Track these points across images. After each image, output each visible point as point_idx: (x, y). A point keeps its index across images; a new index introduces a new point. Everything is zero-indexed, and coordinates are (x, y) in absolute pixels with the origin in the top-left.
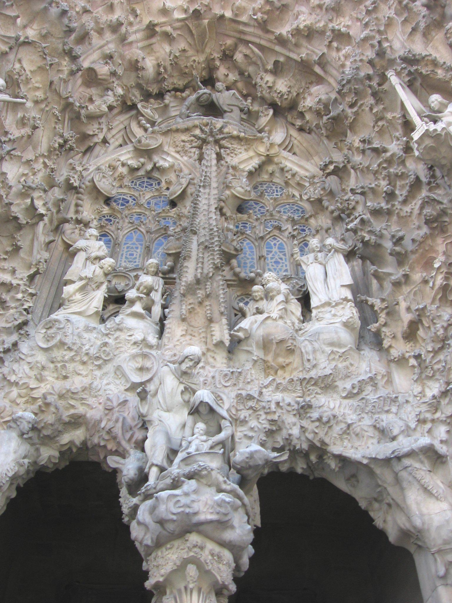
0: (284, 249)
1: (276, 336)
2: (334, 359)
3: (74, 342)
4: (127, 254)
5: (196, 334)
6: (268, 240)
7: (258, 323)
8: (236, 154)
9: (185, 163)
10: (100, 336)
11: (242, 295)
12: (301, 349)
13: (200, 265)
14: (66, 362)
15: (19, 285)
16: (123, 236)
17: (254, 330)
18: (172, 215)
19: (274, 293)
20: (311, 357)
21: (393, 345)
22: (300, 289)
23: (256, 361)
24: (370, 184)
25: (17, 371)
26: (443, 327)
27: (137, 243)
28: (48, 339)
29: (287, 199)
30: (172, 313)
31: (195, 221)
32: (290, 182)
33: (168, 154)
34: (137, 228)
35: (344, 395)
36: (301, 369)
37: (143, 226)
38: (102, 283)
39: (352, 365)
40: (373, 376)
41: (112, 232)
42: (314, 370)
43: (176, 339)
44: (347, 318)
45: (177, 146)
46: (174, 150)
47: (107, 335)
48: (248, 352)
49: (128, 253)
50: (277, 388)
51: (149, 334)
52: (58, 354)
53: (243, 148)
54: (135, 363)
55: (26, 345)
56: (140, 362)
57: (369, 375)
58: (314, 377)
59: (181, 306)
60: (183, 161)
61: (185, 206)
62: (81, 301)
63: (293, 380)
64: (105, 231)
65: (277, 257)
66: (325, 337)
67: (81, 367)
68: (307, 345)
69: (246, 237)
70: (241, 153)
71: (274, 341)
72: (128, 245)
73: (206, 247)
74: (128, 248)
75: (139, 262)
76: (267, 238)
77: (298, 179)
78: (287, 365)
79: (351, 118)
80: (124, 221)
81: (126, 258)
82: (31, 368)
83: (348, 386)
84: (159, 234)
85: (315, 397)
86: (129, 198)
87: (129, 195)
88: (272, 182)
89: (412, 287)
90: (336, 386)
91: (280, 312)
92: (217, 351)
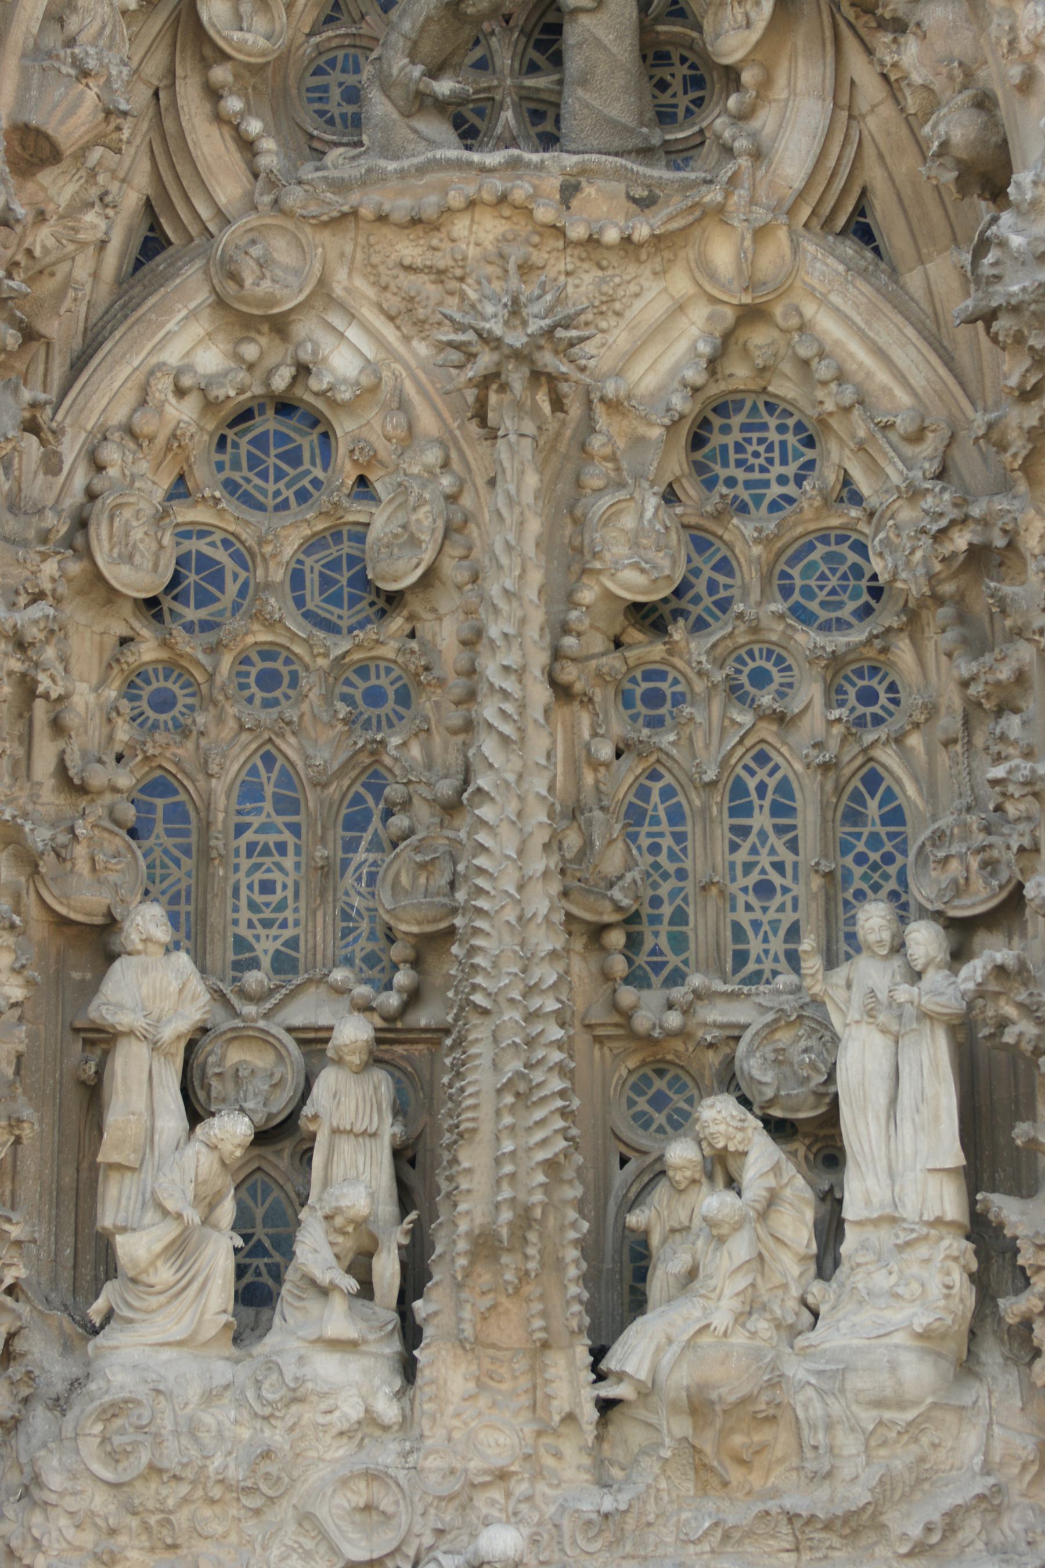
0: (791, 811)
1: (724, 1391)
2: (884, 1444)
3: (185, 1460)
4: (250, 887)
7: (676, 1348)
8: (618, 314)
9: (422, 377)
11: (644, 1064)
12: (794, 1410)
13: (506, 1193)
14: (171, 1512)
16: (228, 795)
17: (662, 1376)
18: (391, 655)
19: (725, 1230)
22: (822, 1089)
23: (667, 1460)
25: (45, 1542)
27: (279, 820)
28: (114, 1457)
29: (817, 519)
30: (436, 1321)
31: (480, 949)
32: (833, 422)
33: (352, 317)
34: (270, 740)
35: (904, 1550)
36: (794, 1461)
37: (292, 740)
39: (935, 1446)
40: (987, 1492)
41: (184, 772)
42: (827, 1483)
43: (450, 1410)
45: (385, 288)
46: (371, 292)
47: (266, 1418)
48: (649, 1425)
49: (259, 876)
50: (726, 1537)
52: (148, 1493)
53: (647, 271)
54: (349, 1495)
55: (55, 1463)
56: (360, 1493)
57: (981, 1485)
58: (821, 1515)
59: (459, 1304)
60: (413, 363)
61: (434, 610)
63: (767, 1513)
64: (160, 767)
65: (764, 860)
66: (860, 1385)
67: (207, 1512)
68: (810, 1400)
69: (658, 761)
70: (637, 295)
71: (718, 1408)
72: (249, 836)
73: (518, 1095)
74: (251, 847)
75: (297, 923)
76: (733, 761)
77: (862, 433)
79: (1015, 456)
80: (220, 720)
81: (253, 906)
82: (78, 1527)
83: (916, 1531)
84: (353, 774)
85: (826, 1557)
86: (221, 555)
87: (217, 537)
88: (764, 390)
90: (884, 1526)
91: (736, 1304)
92: (564, 1430)
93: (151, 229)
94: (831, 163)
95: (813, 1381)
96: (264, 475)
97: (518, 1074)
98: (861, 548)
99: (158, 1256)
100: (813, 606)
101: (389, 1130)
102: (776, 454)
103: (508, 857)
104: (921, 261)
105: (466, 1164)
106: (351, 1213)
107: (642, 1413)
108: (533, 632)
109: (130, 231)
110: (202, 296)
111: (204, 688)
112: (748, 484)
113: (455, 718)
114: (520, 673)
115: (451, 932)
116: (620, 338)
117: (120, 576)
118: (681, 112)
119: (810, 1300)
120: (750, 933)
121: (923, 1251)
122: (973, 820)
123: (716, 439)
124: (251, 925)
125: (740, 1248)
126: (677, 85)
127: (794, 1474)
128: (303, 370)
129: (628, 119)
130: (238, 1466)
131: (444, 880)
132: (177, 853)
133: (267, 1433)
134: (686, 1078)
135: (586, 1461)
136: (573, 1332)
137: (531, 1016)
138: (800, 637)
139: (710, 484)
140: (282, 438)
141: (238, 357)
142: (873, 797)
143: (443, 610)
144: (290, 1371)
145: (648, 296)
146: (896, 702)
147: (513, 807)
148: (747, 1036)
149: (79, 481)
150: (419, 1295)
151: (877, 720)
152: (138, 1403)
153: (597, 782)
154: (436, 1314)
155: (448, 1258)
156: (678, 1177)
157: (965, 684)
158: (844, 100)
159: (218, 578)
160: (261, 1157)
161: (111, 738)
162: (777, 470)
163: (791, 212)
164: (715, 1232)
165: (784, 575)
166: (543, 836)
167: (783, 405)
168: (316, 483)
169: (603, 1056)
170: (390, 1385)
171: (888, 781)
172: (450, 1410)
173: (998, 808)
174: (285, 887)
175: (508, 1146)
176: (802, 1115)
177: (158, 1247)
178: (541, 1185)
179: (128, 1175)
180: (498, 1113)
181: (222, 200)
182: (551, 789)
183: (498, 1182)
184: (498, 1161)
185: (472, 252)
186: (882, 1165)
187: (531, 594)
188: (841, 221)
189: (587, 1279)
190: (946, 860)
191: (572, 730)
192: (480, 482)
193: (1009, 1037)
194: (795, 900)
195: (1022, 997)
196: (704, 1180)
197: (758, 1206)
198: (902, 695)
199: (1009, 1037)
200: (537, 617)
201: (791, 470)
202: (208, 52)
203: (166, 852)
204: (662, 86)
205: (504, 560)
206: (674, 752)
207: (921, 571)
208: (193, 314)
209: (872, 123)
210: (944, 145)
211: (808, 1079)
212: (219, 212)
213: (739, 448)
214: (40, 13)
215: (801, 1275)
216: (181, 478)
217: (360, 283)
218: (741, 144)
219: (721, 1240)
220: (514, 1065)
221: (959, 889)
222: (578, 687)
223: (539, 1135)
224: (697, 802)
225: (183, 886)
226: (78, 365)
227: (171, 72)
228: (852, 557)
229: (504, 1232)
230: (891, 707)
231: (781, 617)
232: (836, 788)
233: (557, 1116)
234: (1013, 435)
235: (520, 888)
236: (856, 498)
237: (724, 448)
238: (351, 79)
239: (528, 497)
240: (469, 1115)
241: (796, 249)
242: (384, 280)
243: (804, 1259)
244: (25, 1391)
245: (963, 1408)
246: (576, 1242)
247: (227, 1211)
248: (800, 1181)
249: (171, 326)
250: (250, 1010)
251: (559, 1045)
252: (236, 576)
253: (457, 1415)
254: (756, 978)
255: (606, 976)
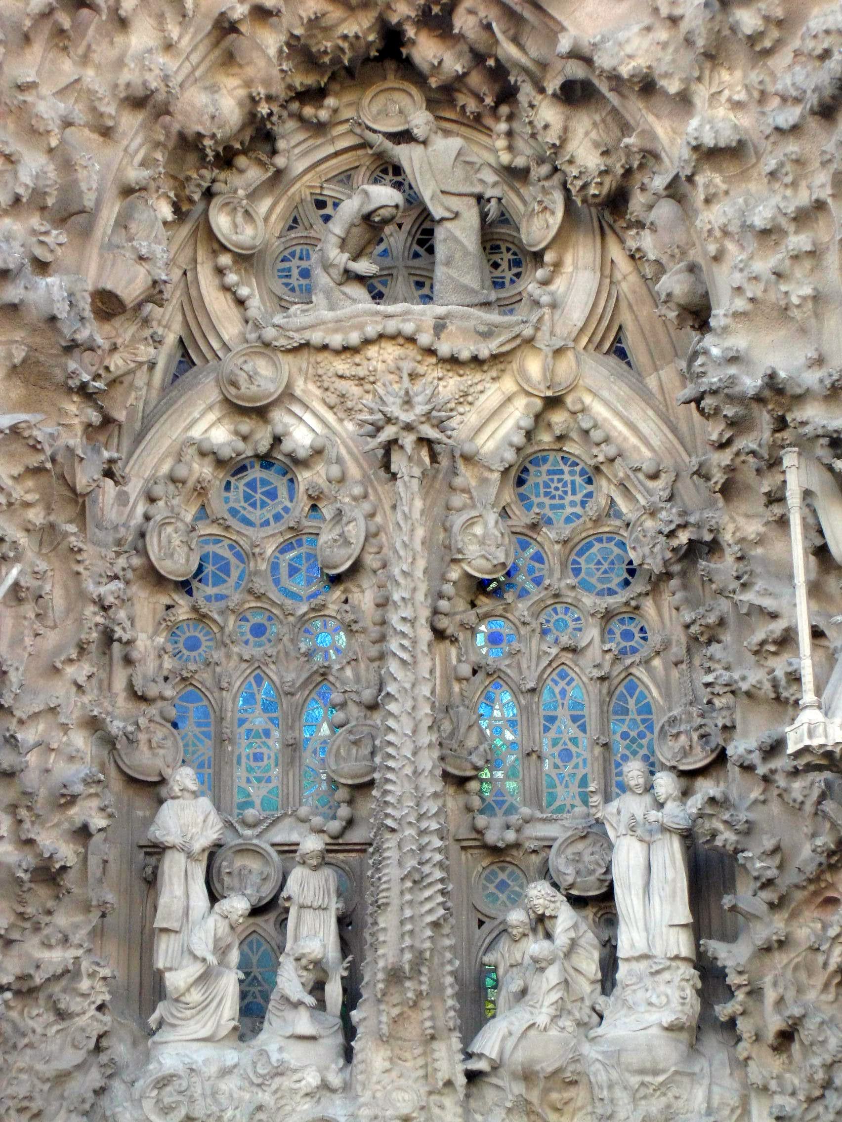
1: (544, 1065)
2: (645, 1097)
5: (408, 1055)
6: (549, 682)
8: (471, 404)
9: (351, 444)
10: (247, 1084)
15: (77, 958)
18: (334, 614)
19: (543, 965)
20: (605, 1094)
21: (754, 1055)
22: (602, 877)
24: (744, 678)
26: (824, 1065)
30: (365, 1023)
31: (390, 791)
32: (603, 467)
33: (307, 407)
36: (589, 1109)
37: (273, 667)
38: (229, 947)
39: (676, 1098)
41: (207, 689)
44: (669, 1020)
45: (327, 389)
46: (318, 392)
47: (259, 1085)
48: (498, 1087)
51: (327, 1068)
53: (488, 376)
59: (380, 1012)
60: (344, 435)
61: (359, 586)
62: (203, 1007)
64: (191, 684)
68: (598, 1070)
70: (482, 392)
71: (541, 1075)
73: (415, 882)
76: (545, 676)
77: (621, 474)
78: (566, 1103)
80: (228, 656)
81: (250, 770)
84: (311, 687)
86: (227, 554)
88: (561, 450)
89: (792, 955)
91: (552, 1011)
92: (446, 1091)
93: (183, 356)
94: (600, 310)
95: (600, 1058)
96: (254, 505)
97: (414, 868)
98: (622, 545)
99: (192, 985)
100: (593, 581)
101: (335, 906)
102: (569, 489)
103: (406, 735)
104: (656, 369)
105: (382, 925)
106: (312, 957)
107: (494, 1080)
108: (420, 596)
109: (170, 357)
110: (214, 396)
111: (218, 635)
112: (553, 507)
113: (374, 651)
114: (412, 622)
115: (371, 784)
116: (473, 418)
117: (165, 567)
118: (507, 281)
119: (598, 1008)
120: (557, 782)
121: (666, 976)
122: (694, 710)
123: (531, 480)
124: (248, 781)
125: (553, 975)
126: (504, 265)
127: (589, 1117)
128: (277, 440)
129: (476, 286)
130: (242, 1116)
131: (366, 751)
132: (202, 736)
133: (260, 1094)
134: (517, 871)
135: (459, 1110)
136: (450, 1030)
137: (422, 833)
138: (584, 600)
139: (529, 507)
140: (264, 482)
141: (237, 433)
142: (631, 697)
143: (365, 586)
144: (275, 1057)
145: (488, 393)
146: (644, 639)
147: (409, 704)
148: (556, 845)
149: (140, 510)
150: (354, 1007)
151: (634, 651)
152: (179, 1077)
153: (461, 689)
154: (365, 1019)
155: (372, 983)
156: (515, 932)
157: (687, 627)
158: (607, 272)
159: (226, 569)
160: (254, 924)
161: (161, 666)
162: (569, 498)
163: (576, 340)
164: (538, 966)
165: (575, 562)
166: (428, 722)
167: (573, 459)
168: (286, 510)
169: (467, 859)
170: (336, 1063)
171: (641, 688)
172: (374, 1079)
173: (709, 702)
174: (269, 758)
175: (408, 913)
176: (591, 894)
177: (191, 980)
178: (430, 937)
179: (173, 935)
180: (402, 893)
181: (226, 338)
182: (433, 692)
183: (403, 935)
184: (402, 923)
185: (380, 366)
186: (641, 924)
187: (419, 573)
188: (606, 346)
189: (458, 996)
190: (678, 735)
191: (446, 659)
192: (387, 507)
193: (719, 842)
194: (585, 761)
195: (726, 816)
196: (531, 934)
197: (565, 950)
198: (649, 635)
199: (719, 842)
200: (423, 588)
201: (578, 498)
202: (216, 246)
203: (195, 736)
204: (496, 266)
205: (402, 553)
206: (508, 671)
207: (659, 557)
208: (210, 408)
209: (624, 287)
210: (669, 295)
211: (594, 871)
212: (225, 346)
213: (547, 485)
214: (112, 222)
215: (592, 992)
216: (203, 506)
217: (311, 387)
218: (545, 299)
219: (542, 970)
220: (412, 863)
221: (686, 752)
222: (449, 632)
223: (428, 906)
224: (523, 702)
225: (206, 757)
226: (139, 438)
227: (195, 261)
228: (617, 551)
229: (407, 967)
230: (642, 642)
231: (574, 587)
232: (609, 693)
233: (439, 895)
234: (715, 471)
235: (415, 754)
236: (619, 515)
237: (537, 485)
238: (304, 264)
239: (416, 515)
240: (384, 894)
241: (578, 363)
242: (326, 385)
243: (593, 982)
244: (109, 1072)
245: (694, 1074)
246: (452, 973)
247: (234, 956)
248: (590, 935)
249: (196, 415)
250: (248, 832)
251: (439, 850)
252: (238, 567)
253: (379, 1082)
254: (560, 809)
255: (469, 809)
